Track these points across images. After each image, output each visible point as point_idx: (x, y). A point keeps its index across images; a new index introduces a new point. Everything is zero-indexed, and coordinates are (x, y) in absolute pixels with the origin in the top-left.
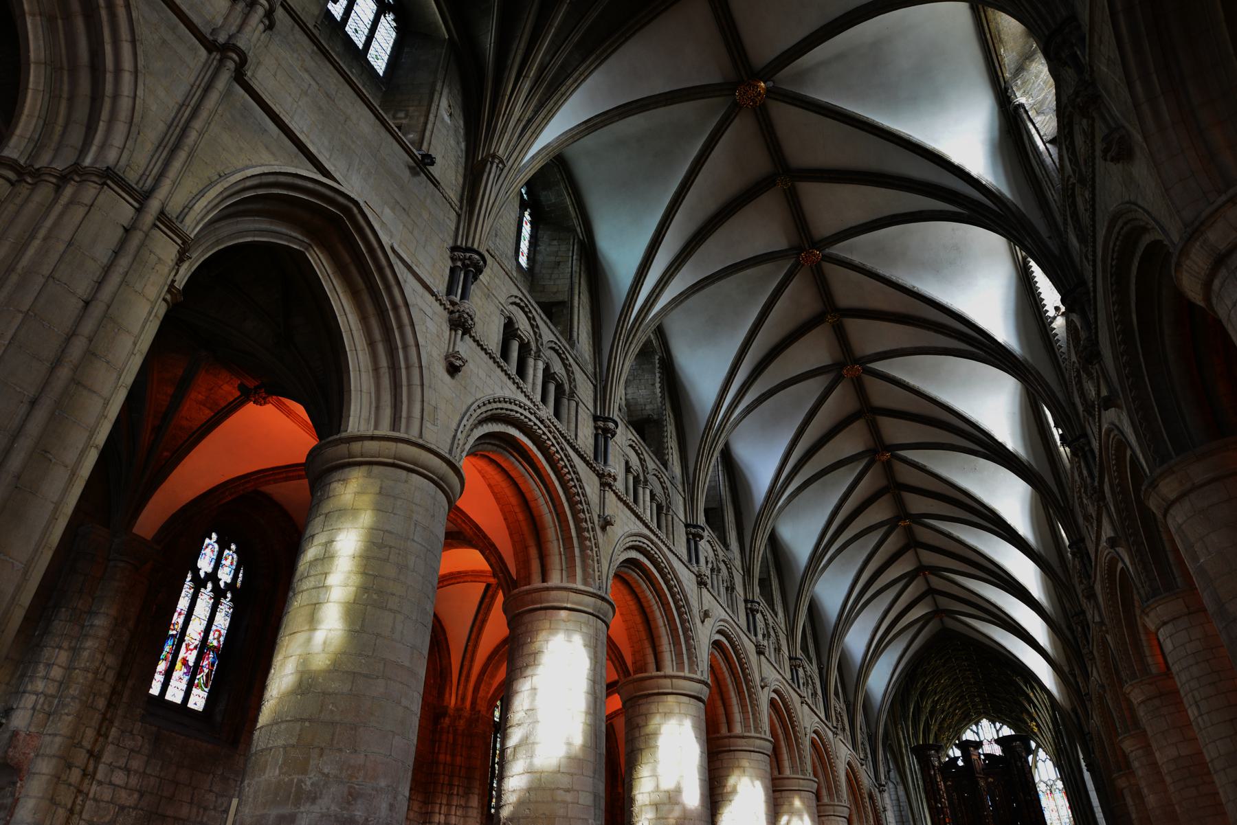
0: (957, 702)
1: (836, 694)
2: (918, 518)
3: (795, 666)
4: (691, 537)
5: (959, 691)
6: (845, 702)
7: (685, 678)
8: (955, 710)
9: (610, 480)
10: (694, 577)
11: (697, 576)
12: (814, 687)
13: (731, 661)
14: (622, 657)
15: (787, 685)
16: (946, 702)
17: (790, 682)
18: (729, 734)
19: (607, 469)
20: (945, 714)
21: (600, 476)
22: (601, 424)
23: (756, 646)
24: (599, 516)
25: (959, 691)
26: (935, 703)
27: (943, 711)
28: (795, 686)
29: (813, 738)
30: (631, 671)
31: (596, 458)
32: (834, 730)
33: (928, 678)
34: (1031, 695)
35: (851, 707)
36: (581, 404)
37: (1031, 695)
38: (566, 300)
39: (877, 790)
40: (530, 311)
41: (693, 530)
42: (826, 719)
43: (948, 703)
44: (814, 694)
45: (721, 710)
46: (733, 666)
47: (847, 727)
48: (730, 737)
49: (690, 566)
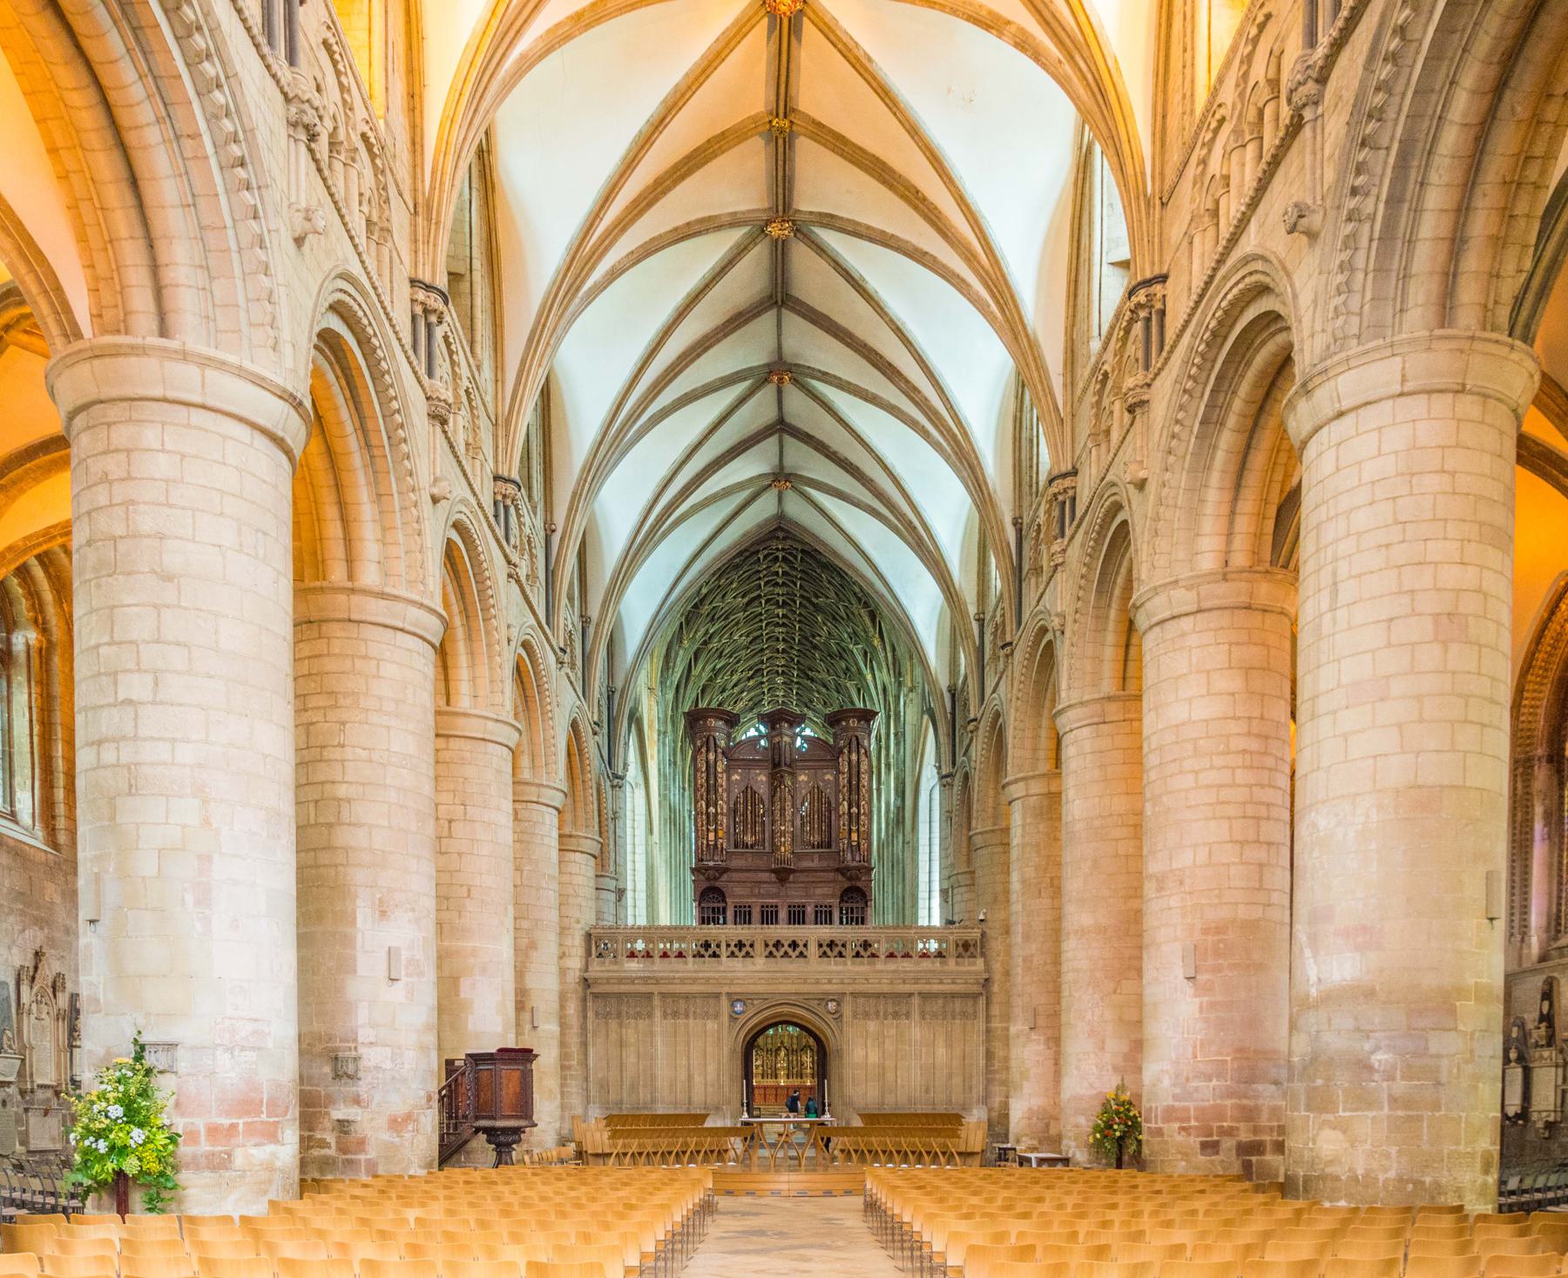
0: (749, 679)
1: (570, 598)
3: (505, 496)
5: (756, 659)
6: (582, 616)
8: (742, 692)
12: (533, 563)
13: (367, 412)
15: (485, 525)
16: (732, 675)
17: (492, 519)
20: (725, 694)
23: (428, 399)
25: (756, 659)
26: (716, 673)
27: (723, 691)
28: (500, 533)
29: (519, 655)
32: (560, 653)
33: (716, 627)
34: (869, 677)
35: (591, 630)
37: (869, 677)
39: (608, 783)
42: (548, 623)
43: (735, 678)
44: (531, 576)
45: (334, 530)
46: (370, 425)
47: (579, 662)
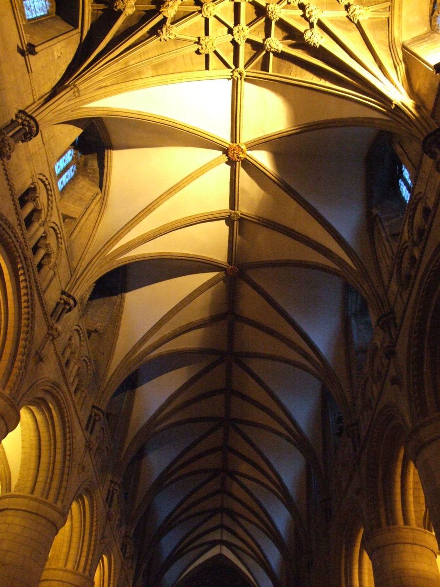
2: (233, 474)
4: (93, 414)
7: (50, 506)
9: (55, 333)
10: (85, 440)
11: (87, 441)
14: (10, 478)
18: (65, 569)
19: (56, 325)
21: (50, 328)
22: (65, 297)
24: (36, 352)
30: (13, 490)
31: (52, 316)
36: (57, 276)
38: (77, 217)
40: (52, 196)
41: (96, 411)
48: (66, 571)
49: (85, 432)
